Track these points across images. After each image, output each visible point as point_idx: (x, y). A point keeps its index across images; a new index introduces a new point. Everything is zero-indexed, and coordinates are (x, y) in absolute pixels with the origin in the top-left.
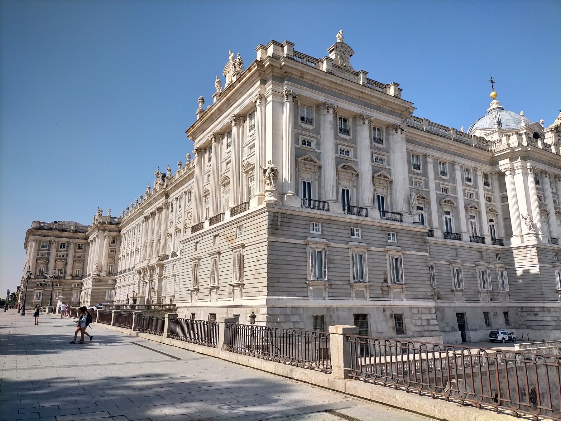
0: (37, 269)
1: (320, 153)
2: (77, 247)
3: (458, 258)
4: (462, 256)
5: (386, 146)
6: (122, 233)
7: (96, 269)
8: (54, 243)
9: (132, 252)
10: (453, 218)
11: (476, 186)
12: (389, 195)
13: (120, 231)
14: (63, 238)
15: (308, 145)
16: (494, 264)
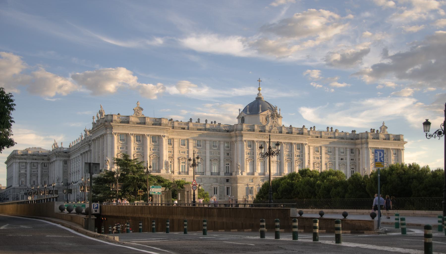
0: (20, 180)
1: (127, 151)
2: (43, 166)
3: (202, 182)
4: (204, 181)
5: (158, 143)
6: (71, 158)
7: (57, 181)
8: (29, 164)
9: (77, 172)
10: (202, 165)
11: (219, 149)
12: (158, 162)
13: (69, 157)
14: (34, 159)
15: (123, 149)
16: (223, 184)
